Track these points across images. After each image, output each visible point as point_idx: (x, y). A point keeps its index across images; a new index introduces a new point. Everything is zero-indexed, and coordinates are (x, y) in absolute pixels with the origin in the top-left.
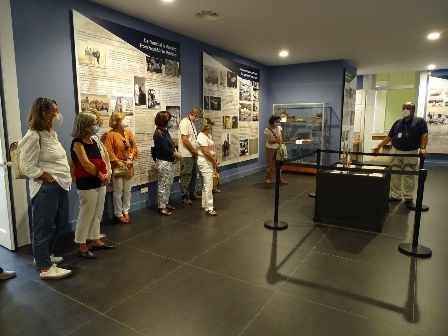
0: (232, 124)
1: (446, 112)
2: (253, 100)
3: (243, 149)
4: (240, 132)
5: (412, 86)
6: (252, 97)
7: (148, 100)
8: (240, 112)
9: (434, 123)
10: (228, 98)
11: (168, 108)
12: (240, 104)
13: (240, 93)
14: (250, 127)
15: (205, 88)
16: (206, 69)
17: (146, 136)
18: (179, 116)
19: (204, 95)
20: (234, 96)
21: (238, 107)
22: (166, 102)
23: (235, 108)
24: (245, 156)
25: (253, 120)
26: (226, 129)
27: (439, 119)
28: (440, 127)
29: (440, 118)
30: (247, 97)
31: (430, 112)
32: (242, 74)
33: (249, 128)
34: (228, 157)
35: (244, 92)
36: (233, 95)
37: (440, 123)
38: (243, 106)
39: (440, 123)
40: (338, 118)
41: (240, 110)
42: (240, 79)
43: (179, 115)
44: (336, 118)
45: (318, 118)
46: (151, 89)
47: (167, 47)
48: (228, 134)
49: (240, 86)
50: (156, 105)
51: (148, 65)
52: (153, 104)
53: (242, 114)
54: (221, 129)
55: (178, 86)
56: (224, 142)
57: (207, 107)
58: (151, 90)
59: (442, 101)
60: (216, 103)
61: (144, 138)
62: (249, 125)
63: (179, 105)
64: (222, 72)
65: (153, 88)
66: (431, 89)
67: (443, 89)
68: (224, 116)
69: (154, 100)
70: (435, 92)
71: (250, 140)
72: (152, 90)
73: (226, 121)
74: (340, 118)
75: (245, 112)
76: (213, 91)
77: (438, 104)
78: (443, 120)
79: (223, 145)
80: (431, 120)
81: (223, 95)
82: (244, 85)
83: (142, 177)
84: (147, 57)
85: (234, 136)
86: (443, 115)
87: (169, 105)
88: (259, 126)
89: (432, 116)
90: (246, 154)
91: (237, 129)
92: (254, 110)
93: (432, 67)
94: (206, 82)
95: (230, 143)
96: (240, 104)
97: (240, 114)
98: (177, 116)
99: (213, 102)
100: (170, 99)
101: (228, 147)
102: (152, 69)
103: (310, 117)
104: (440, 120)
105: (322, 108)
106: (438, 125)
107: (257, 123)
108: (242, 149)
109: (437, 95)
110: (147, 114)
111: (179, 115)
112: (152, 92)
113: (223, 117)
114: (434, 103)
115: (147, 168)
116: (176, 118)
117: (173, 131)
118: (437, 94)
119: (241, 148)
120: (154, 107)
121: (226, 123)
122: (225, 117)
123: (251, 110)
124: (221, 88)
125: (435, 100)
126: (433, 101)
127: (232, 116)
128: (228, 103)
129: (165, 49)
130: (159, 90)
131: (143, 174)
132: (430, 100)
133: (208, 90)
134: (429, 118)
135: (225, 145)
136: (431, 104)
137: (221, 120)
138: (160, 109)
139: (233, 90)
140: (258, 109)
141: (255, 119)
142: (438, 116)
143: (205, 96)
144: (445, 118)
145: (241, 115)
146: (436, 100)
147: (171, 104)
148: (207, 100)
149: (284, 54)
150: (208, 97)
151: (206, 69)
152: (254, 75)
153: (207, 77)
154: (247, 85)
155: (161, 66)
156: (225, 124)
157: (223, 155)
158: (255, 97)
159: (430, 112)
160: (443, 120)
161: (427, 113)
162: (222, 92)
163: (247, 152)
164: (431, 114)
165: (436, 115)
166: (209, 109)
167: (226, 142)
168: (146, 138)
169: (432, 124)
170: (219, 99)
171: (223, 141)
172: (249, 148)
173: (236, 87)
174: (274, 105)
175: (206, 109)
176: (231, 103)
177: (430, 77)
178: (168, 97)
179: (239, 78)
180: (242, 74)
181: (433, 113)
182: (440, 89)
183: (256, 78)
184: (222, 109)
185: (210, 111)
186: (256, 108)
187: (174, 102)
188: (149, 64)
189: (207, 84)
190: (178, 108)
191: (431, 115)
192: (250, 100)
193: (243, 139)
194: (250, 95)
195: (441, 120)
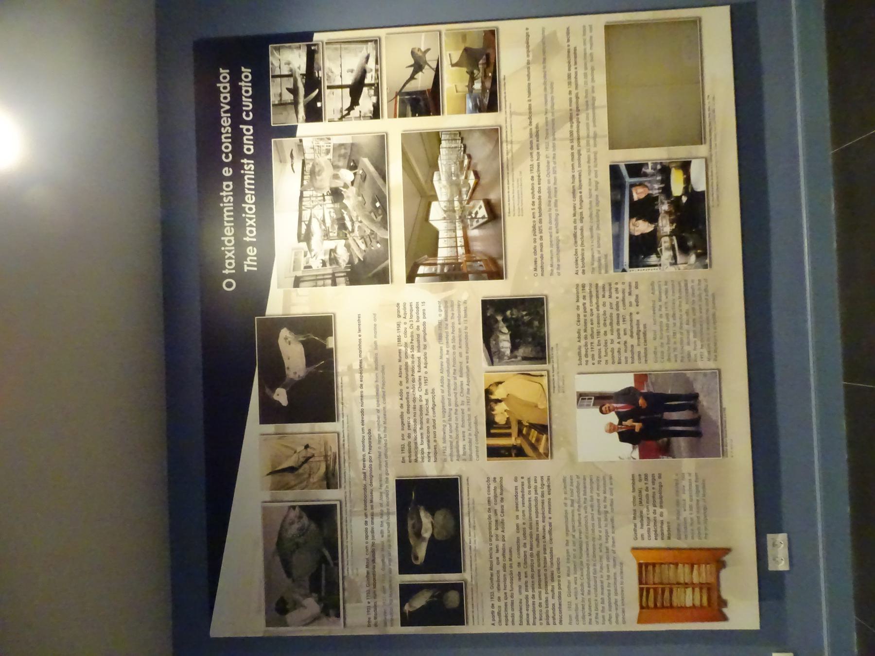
0: (525, 359)
2: (376, 114)
10: (393, 404)
20: (375, 343)
25: (492, 105)
26: (554, 426)
34: (704, 401)
36: (371, 360)
42: (279, 286)
64: (273, 473)
71: (613, 146)
73: (508, 425)
91: (550, 299)
96: (411, 278)
97: (464, 277)
99: (422, 551)
101: (647, 396)
108: (665, 242)
119: (659, 256)
122: (489, 435)
123: (436, 137)
124: (350, 473)
128: (418, 404)
133: (375, 597)
148: (420, 601)
150: (407, 592)
154: (301, 197)
156: (526, 437)
157: (695, 452)
166: (459, 587)
167: (622, 417)
175: (458, 616)
176: (417, 375)
184: (451, 470)
185: (466, 575)
189: (348, 606)
192: (382, 140)
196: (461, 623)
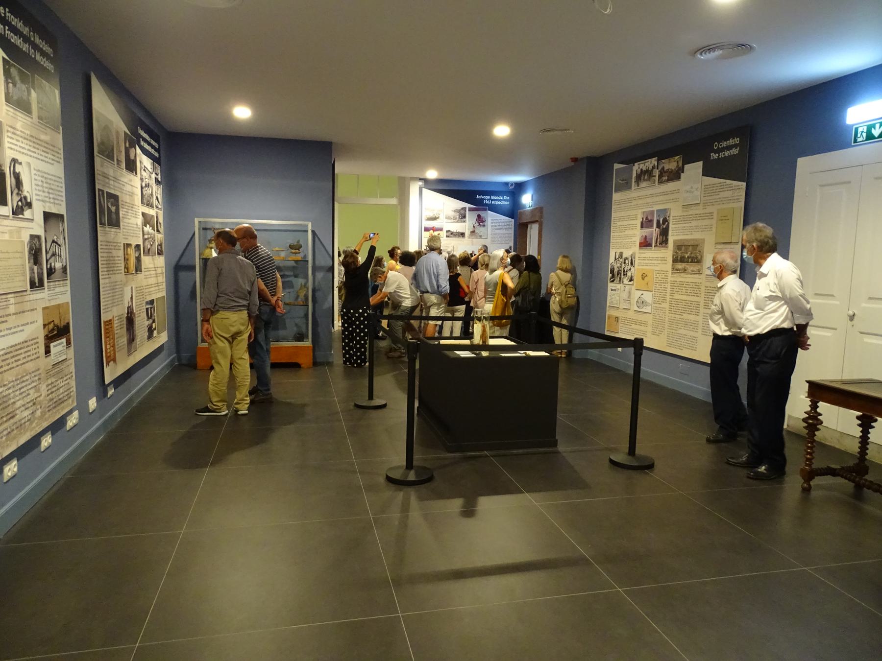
1: (448, 247)
2: (156, 207)
3: (151, 321)
4: (144, 283)
5: (394, 201)
6: (155, 202)
7: (12, 193)
8: (143, 231)
11: (47, 216)
12: (143, 214)
13: (142, 188)
14: (155, 268)
15: (97, 170)
16: (98, 121)
17: (12, 301)
18: (64, 241)
19: (97, 187)
21: (140, 220)
22: (43, 201)
23: (137, 225)
24: (154, 339)
25: (158, 253)
30: (149, 198)
32: (142, 143)
33: (154, 272)
35: (146, 186)
38: (147, 220)
40: (327, 252)
41: (143, 228)
42: (140, 153)
43: (64, 239)
44: (325, 252)
45: (294, 251)
46: (16, 157)
47: (38, 41)
48: (132, 287)
49: (141, 170)
50: (27, 207)
51: (7, 83)
52: (20, 203)
53: (146, 239)
54: (121, 277)
55: (47, 157)
56: (128, 308)
57: (103, 221)
58: (14, 161)
59: (441, 229)
60: (113, 209)
61: (7, 307)
62: (154, 264)
63: (62, 209)
65: (20, 158)
68: (125, 243)
69: (22, 192)
70: (431, 215)
72: (17, 160)
74: (331, 254)
75: (148, 234)
76: (108, 178)
79: (126, 315)
81: (121, 189)
82: (144, 170)
83: (9, 430)
84: (3, 58)
85: (140, 290)
86: (444, 251)
87: (47, 210)
88: (164, 266)
90: (154, 336)
92: (158, 231)
93: (432, 174)
94: (99, 153)
95: (134, 312)
96: (143, 214)
98: (62, 242)
99: (110, 206)
100: (49, 193)
102: (15, 98)
103: (277, 249)
105: (307, 231)
107: (161, 261)
109: (435, 219)
110: (11, 232)
111: (64, 239)
112: (18, 169)
113: (124, 244)
114: (432, 231)
115: (18, 398)
116: (60, 246)
117: (57, 283)
118: (434, 217)
120: (23, 214)
121: (128, 259)
123: (154, 231)
125: (432, 226)
127: (134, 244)
129: (35, 47)
130: (29, 164)
131: (12, 421)
135: (129, 315)
137: (121, 253)
138: (33, 220)
139: (131, 176)
140: (162, 227)
141: (160, 253)
143: (99, 190)
145: (144, 240)
147: (50, 207)
149: (242, 112)
151: (98, 121)
152: (153, 147)
153: (99, 140)
155: (29, 94)
158: (157, 199)
162: (121, 182)
163: (155, 329)
166: (105, 224)
167: (130, 307)
168: (12, 309)
170: (114, 199)
171: (127, 306)
172: (156, 320)
173: (136, 174)
174: (196, 220)
177: (423, 189)
178: (45, 185)
179: (139, 151)
180: (142, 143)
183: (157, 154)
185: (107, 229)
186: (160, 224)
187: (56, 202)
188: (9, 81)
190: (62, 216)
192: (152, 206)
193: (149, 299)
194: (152, 195)
196: (100, 224)
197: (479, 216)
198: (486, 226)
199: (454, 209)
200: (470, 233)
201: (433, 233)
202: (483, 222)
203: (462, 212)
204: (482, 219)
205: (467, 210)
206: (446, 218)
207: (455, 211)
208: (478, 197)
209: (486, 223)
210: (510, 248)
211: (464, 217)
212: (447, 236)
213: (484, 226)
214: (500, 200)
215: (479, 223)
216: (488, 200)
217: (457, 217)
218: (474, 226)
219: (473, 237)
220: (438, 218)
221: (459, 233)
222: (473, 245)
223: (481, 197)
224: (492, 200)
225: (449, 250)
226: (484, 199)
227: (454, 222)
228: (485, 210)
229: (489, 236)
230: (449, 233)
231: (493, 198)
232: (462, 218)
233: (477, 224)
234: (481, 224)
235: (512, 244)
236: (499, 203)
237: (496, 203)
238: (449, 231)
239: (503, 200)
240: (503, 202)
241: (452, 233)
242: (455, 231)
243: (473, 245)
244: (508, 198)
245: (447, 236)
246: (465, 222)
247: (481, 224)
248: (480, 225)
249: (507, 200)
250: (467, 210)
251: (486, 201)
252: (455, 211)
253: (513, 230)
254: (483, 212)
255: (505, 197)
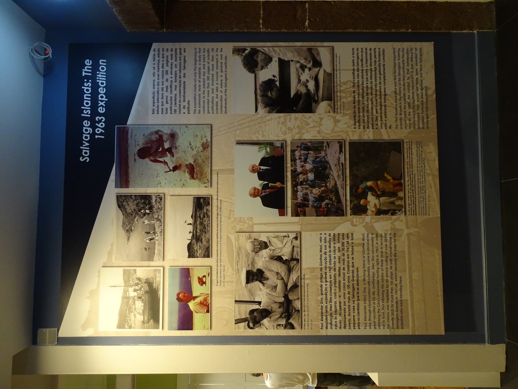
9: (290, 297)
27: (273, 279)
28: (312, 270)
29: (267, 274)
31: (238, 321)
37: (290, 270)
39: (290, 270)
66: (121, 325)
67: (127, 275)
77: (197, 290)
78: (279, 259)
80: (278, 311)
86: (253, 263)
89: (256, 307)
104: (277, 273)
106: (300, 278)
114: (192, 305)
118: (146, 297)
125: (176, 304)
126: (180, 310)
132: (176, 324)
134: (265, 321)
136: (198, 318)
142: (257, 284)
144: (265, 253)
146: (178, 299)
159: (238, 321)
160: (279, 259)
161: (242, 330)
164: (245, 314)
165: (251, 293)
169: (297, 304)
181: (243, 306)
182: (127, 283)
191: (252, 312)
195: (277, 267)
197: (143, 153)
198: (177, 130)
199: (123, 233)
200: (195, 182)
201: (198, 300)
202: (160, 140)
203: (131, 206)
204: (152, 141)
205: (124, 191)
206: (150, 258)
207: (129, 231)
208: (85, 157)
209: (166, 131)
210: (238, 51)
211: (146, 199)
212: (207, 254)
213: (173, 136)
214: (95, 87)
215: (164, 153)
216: (93, 126)
217: (146, 222)
218: (175, 169)
219: (207, 170)
220: (149, 283)
221: (195, 216)
222: (231, 171)
223: (85, 149)
224: (94, 111)
225: (249, 246)
226: (93, 140)
227: (163, 232)
228: (124, 133)
229: (206, 118)
230: (196, 247)
231: (87, 112)
232: (151, 208)
233: (168, 158)
234: (167, 145)
235: (228, 47)
236: (102, 91)
237: (102, 99)
238: (190, 247)
239: (93, 78)
240: (101, 78)
241: (196, 238)
242: (191, 228)
243: (231, 171)
244: (88, 63)
245: (207, 254)
246: (161, 198)
247: (167, 145)
248: (170, 150)
249: (95, 68)
250: (124, 191)
251: (99, 131)
252: (129, 231)
253: (184, 45)
254: (130, 141)
255: (86, 71)
